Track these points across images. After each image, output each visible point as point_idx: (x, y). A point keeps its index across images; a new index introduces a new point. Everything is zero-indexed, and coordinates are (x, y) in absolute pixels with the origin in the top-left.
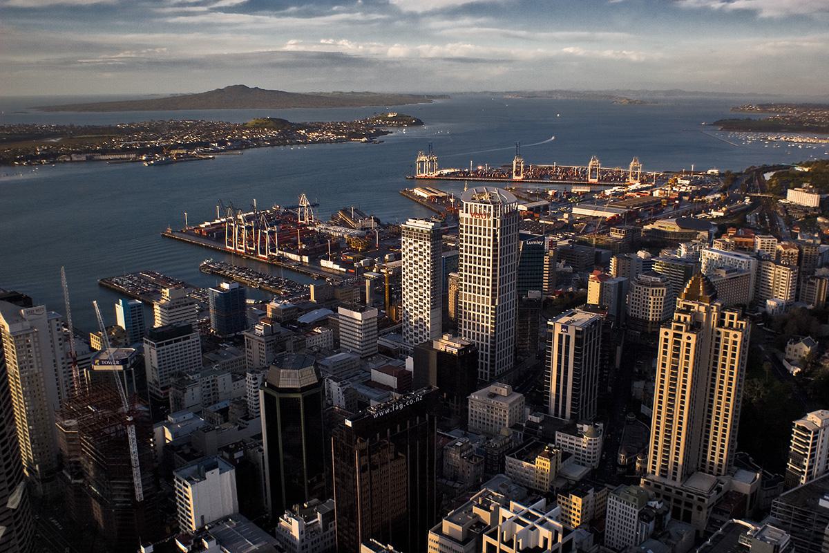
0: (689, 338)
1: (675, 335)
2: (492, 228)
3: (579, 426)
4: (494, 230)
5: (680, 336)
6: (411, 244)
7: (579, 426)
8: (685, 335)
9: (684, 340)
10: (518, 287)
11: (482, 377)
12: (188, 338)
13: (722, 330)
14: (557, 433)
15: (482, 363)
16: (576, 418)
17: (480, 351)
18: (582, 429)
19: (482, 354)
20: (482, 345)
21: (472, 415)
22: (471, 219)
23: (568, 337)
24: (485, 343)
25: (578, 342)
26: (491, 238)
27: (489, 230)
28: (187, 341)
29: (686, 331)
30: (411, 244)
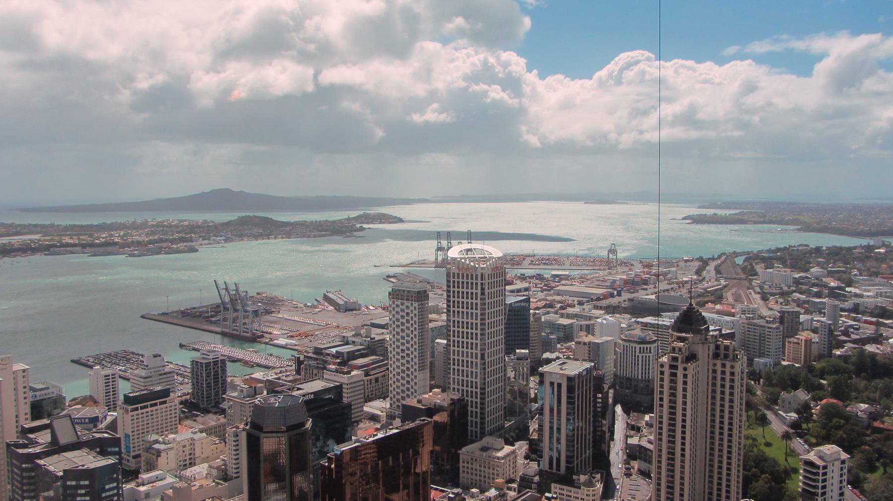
0: (685, 369)
1: (671, 367)
2: (479, 282)
3: (575, 477)
4: (482, 284)
5: (676, 367)
6: (397, 306)
7: (575, 477)
8: (681, 367)
9: (680, 372)
10: (506, 333)
11: (472, 436)
12: (165, 402)
13: (719, 363)
14: (553, 485)
15: (472, 421)
16: (570, 471)
17: (469, 409)
18: (579, 480)
19: (472, 412)
20: (472, 402)
21: (464, 472)
22: (458, 274)
23: (559, 385)
24: (474, 390)
25: (570, 389)
26: (479, 291)
27: (477, 284)
28: (164, 406)
29: (682, 362)
30: (397, 306)
